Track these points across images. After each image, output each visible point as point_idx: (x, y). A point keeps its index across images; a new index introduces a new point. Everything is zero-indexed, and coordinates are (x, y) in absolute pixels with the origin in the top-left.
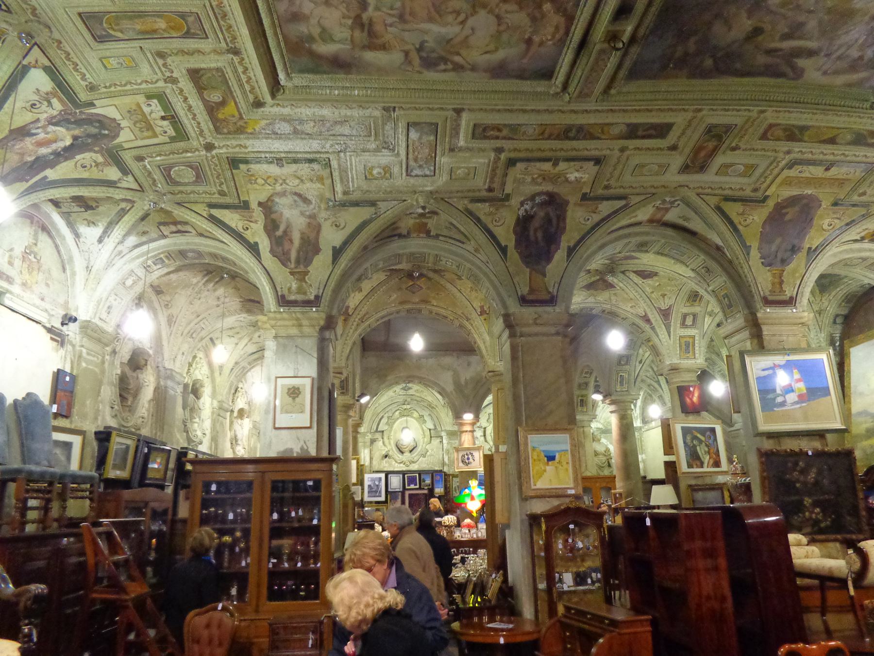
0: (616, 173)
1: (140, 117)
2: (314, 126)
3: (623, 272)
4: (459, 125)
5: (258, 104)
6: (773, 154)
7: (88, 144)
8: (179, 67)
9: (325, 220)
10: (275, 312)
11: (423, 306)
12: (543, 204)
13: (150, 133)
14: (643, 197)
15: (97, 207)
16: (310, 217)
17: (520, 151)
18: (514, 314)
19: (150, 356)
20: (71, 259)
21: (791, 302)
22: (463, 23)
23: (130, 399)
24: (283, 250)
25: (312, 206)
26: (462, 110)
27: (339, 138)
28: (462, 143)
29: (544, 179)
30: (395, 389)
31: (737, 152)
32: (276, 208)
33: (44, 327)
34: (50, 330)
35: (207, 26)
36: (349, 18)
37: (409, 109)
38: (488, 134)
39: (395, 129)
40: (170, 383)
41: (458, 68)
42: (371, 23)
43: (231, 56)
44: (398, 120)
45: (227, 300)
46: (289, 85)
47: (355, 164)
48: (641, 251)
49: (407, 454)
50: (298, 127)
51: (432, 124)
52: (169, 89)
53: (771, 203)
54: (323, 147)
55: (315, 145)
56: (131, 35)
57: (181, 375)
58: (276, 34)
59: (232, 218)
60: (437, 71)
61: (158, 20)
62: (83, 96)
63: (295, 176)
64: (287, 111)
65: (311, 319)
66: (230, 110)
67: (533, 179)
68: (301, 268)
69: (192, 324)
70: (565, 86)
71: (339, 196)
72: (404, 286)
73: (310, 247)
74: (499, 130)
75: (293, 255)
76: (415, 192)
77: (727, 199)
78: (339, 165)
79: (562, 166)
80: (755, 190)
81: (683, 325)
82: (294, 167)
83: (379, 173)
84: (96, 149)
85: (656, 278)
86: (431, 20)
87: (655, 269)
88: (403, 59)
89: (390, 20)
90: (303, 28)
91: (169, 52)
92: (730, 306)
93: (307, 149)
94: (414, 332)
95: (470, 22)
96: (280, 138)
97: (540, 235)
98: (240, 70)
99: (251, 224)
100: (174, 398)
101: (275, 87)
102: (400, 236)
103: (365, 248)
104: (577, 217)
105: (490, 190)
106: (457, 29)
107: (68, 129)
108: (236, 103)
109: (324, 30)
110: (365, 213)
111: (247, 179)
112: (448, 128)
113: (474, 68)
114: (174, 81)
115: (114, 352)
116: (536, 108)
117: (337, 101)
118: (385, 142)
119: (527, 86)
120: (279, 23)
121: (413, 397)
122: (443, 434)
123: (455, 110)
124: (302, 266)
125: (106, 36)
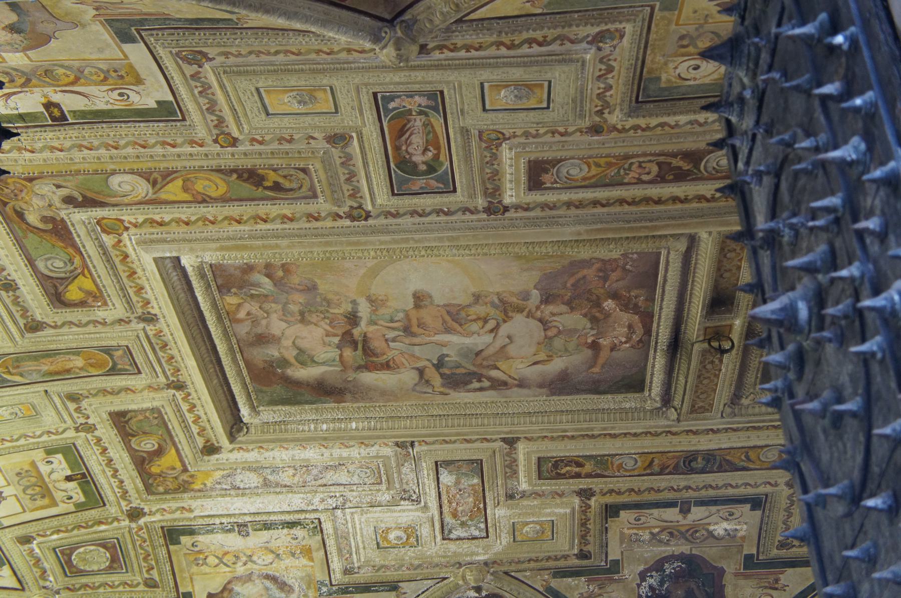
1: (33, 480)
2: (294, 475)
4: (515, 460)
5: (211, 449)
8: (98, 411)
12: (676, 577)
13: (46, 501)
17: (619, 493)
26: (518, 439)
27: (332, 488)
28: (524, 486)
29: (671, 534)
35: (140, 360)
36: (335, 335)
37: (434, 443)
38: (563, 471)
39: (417, 470)
41: (498, 385)
42: (365, 339)
44: (420, 459)
46: (256, 421)
47: (361, 525)
50: (269, 477)
51: (472, 461)
52: (81, 439)
54: (310, 503)
55: (297, 501)
56: (35, 377)
58: (234, 360)
61: (72, 357)
63: (266, 548)
64: (252, 456)
66: (170, 459)
67: (651, 533)
70: (667, 399)
71: (338, 576)
76: (460, 565)
78: (336, 529)
79: (697, 513)
82: (265, 535)
83: (399, 538)
86: (448, 330)
89: (391, 335)
90: (273, 352)
91: (85, 393)
93: (286, 508)
95: (504, 329)
96: (243, 495)
98: (185, 407)
101: (235, 425)
105: (583, 555)
106: (488, 338)
108: (177, 451)
109: (301, 351)
111: (192, 558)
112: (499, 468)
114: (91, 429)
116: (627, 430)
117: (325, 439)
118: (404, 491)
119: (608, 401)
120: (241, 347)
123: (504, 440)
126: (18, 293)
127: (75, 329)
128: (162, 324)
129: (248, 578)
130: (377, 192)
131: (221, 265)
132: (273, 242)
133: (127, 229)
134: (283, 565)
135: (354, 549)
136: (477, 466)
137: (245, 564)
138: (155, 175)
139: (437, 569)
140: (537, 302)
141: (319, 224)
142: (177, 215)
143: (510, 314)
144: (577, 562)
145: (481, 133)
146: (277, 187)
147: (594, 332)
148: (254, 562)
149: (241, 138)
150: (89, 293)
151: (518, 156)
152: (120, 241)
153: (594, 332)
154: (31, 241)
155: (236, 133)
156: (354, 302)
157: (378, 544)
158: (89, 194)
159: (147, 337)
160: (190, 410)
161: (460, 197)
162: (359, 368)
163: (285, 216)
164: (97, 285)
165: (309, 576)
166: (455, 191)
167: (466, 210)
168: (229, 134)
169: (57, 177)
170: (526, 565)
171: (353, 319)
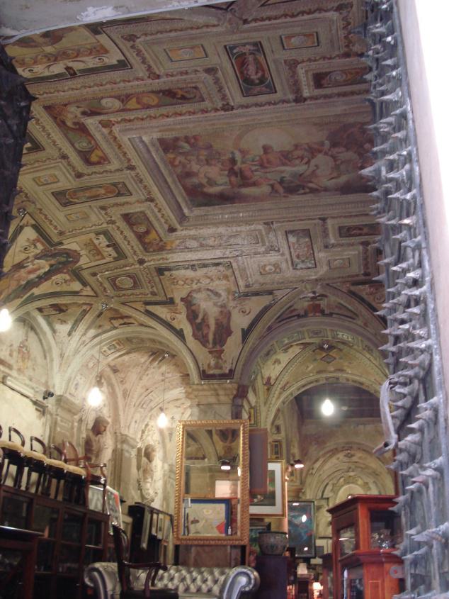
1: (92, 247)
4: (326, 229)
5: (172, 230)
7: (60, 268)
8: (116, 213)
9: (234, 308)
10: (198, 384)
11: (339, 374)
13: (100, 257)
15: (67, 310)
16: (221, 306)
19: (108, 423)
20: (50, 349)
22: (308, 162)
23: (94, 459)
24: (202, 333)
28: (333, 241)
30: (338, 456)
32: (194, 302)
33: (32, 401)
34: (35, 403)
35: (130, 188)
36: (225, 170)
37: (283, 222)
38: (353, 233)
39: (276, 236)
40: (125, 447)
41: (313, 191)
42: (241, 171)
43: (149, 203)
45: (170, 375)
46: (192, 215)
50: (204, 242)
54: (224, 254)
55: (218, 253)
56: (84, 199)
57: (134, 440)
59: (161, 311)
60: (299, 194)
61: (100, 189)
62: (56, 239)
64: (192, 232)
65: (225, 389)
66: (153, 236)
68: (218, 348)
69: (143, 397)
72: (318, 357)
73: (224, 331)
74: (360, 229)
75: (211, 337)
82: (205, 270)
84: (65, 271)
86: (284, 164)
88: (270, 189)
89: (254, 168)
90: (195, 180)
93: (212, 256)
94: (325, 399)
95: (313, 162)
96: (191, 251)
99: (177, 315)
100: (129, 459)
101: (183, 218)
102: (299, 316)
103: (269, 328)
105: (366, 274)
106: (305, 167)
107: (47, 261)
108: (156, 231)
109: (209, 179)
110: (266, 300)
113: (326, 190)
114: (113, 222)
115: (81, 420)
117: (227, 222)
123: (320, 219)
124: (218, 346)
125: (68, 203)
126: (69, 160)
127: (98, 175)
128: (138, 170)
129: (199, 290)
130: (236, 97)
131: (163, 139)
132: (185, 126)
133: (114, 125)
134: (215, 284)
135: (249, 275)
136: (307, 233)
137: (196, 284)
138: (122, 97)
139: (291, 284)
140: (329, 147)
141: (206, 115)
142: (136, 116)
143: (315, 154)
145: (285, 61)
146: (183, 98)
147: (361, 161)
148: (201, 283)
149: (161, 74)
150: (101, 158)
151: (307, 72)
152: (111, 131)
153: (361, 161)
154: (71, 134)
155: (158, 73)
156: (232, 153)
157: (261, 272)
158: (93, 109)
159: (132, 177)
160: (159, 212)
161: (279, 95)
162: (240, 186)
163: (190, 112)
164: (104, 154)
165: (228, 289)
166: (276, 92)
167: (284, 101)
168: (155, 73)
169: (77, 102)
171: (233, 161)
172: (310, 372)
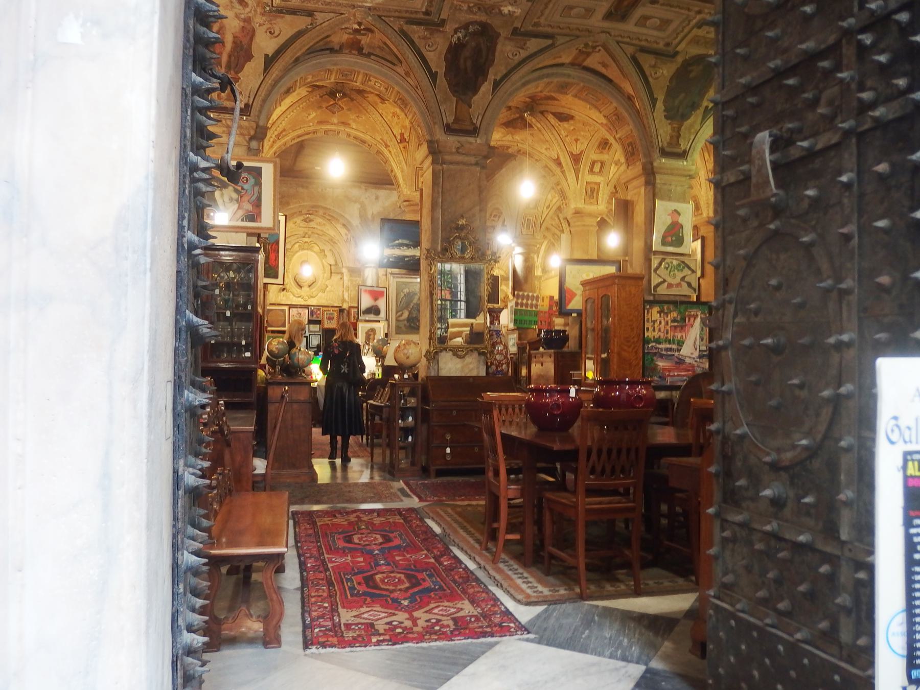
0: (547, 11)
3: (542, 113)
6: (686, 12)
12: (474, 34)
14: (568, 39)
16: (245, 20)
18: (437, 141)
21: (683, 155)
25: (248, 10)
29: (479, 9)
30: (295, 220)
31: (656, 6)
48: (562, 93)
49: (306, 289)
53: (680, 59)
67: (469, 7)
77: (643, 50)
80: (668, 45)
81: (591, 171)
85: (571, 122)
87: (573, 113)
92: (633, 154)
97: (469, 64)
102: (332, 50)
104: (506, 51)
105: (427, 13)
110: (302, 22)
121: (315, 230)
122: (345, 271)
124: (232, 72)
144: (422, 16)
170: (393, 14)
172: (309, 121)
